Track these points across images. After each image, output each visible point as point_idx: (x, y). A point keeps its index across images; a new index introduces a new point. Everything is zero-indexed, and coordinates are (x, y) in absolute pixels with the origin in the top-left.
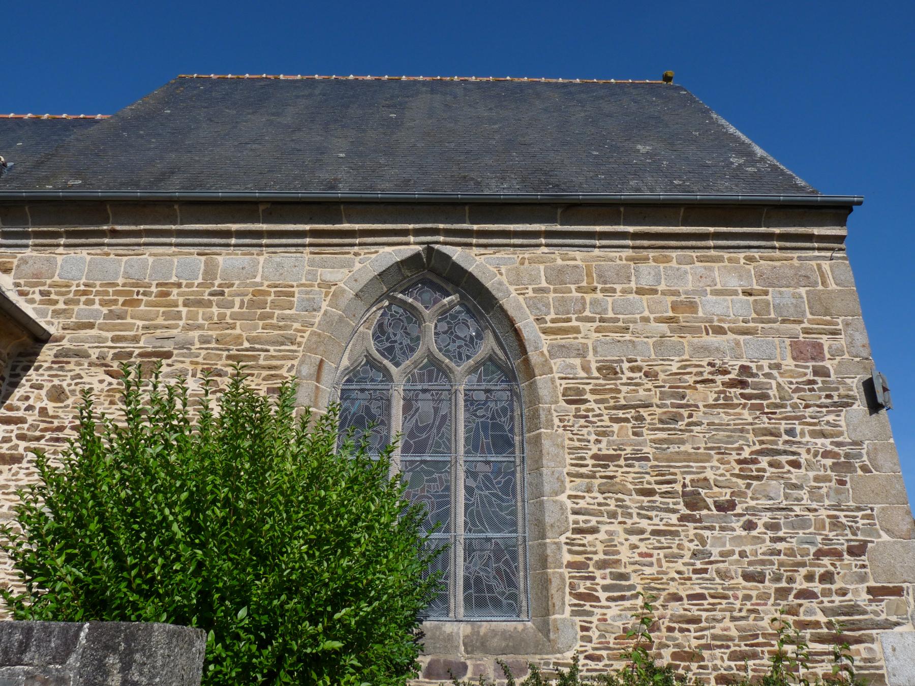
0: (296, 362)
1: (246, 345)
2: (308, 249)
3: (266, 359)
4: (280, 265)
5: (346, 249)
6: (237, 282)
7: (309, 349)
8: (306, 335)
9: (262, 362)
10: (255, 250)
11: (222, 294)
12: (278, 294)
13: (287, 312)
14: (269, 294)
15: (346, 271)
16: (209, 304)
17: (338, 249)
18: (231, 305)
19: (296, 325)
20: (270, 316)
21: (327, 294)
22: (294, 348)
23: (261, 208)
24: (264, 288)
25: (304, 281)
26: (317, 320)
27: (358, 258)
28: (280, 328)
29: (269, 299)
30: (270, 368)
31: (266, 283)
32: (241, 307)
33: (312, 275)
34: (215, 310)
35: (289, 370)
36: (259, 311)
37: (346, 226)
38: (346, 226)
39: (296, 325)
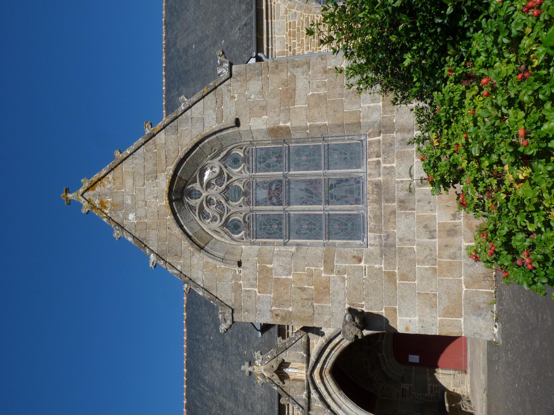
0: (315, 15)
2: (273, 20)
4: (279, 30)
5: (273, 7)
6: (286, 43)
7: (310, 12)
8: (305, 14)
10: (274, 39)
11: (290, 47)
12: (290, 27)
13: (297, 23)
14: (290, 31)
15: (281, 6)
16: (294, 51)
17: (273, 10)
18: (295, 43)
19: (302, 18)
20: (298, 29)
21: (290, 11)
22: (310, 17)
23: (258, 36)
24: (288, 33)
25: (285, 20)
26: (300, 12)
27: (276, 3)
28: (303, 24)
29: (292, 30)
31: (286, 33)
32: (295, 39)
34: (296, 48)
35: (318, 17)
36: (296, 32)
37: (264, 8)
38: (264, 8)
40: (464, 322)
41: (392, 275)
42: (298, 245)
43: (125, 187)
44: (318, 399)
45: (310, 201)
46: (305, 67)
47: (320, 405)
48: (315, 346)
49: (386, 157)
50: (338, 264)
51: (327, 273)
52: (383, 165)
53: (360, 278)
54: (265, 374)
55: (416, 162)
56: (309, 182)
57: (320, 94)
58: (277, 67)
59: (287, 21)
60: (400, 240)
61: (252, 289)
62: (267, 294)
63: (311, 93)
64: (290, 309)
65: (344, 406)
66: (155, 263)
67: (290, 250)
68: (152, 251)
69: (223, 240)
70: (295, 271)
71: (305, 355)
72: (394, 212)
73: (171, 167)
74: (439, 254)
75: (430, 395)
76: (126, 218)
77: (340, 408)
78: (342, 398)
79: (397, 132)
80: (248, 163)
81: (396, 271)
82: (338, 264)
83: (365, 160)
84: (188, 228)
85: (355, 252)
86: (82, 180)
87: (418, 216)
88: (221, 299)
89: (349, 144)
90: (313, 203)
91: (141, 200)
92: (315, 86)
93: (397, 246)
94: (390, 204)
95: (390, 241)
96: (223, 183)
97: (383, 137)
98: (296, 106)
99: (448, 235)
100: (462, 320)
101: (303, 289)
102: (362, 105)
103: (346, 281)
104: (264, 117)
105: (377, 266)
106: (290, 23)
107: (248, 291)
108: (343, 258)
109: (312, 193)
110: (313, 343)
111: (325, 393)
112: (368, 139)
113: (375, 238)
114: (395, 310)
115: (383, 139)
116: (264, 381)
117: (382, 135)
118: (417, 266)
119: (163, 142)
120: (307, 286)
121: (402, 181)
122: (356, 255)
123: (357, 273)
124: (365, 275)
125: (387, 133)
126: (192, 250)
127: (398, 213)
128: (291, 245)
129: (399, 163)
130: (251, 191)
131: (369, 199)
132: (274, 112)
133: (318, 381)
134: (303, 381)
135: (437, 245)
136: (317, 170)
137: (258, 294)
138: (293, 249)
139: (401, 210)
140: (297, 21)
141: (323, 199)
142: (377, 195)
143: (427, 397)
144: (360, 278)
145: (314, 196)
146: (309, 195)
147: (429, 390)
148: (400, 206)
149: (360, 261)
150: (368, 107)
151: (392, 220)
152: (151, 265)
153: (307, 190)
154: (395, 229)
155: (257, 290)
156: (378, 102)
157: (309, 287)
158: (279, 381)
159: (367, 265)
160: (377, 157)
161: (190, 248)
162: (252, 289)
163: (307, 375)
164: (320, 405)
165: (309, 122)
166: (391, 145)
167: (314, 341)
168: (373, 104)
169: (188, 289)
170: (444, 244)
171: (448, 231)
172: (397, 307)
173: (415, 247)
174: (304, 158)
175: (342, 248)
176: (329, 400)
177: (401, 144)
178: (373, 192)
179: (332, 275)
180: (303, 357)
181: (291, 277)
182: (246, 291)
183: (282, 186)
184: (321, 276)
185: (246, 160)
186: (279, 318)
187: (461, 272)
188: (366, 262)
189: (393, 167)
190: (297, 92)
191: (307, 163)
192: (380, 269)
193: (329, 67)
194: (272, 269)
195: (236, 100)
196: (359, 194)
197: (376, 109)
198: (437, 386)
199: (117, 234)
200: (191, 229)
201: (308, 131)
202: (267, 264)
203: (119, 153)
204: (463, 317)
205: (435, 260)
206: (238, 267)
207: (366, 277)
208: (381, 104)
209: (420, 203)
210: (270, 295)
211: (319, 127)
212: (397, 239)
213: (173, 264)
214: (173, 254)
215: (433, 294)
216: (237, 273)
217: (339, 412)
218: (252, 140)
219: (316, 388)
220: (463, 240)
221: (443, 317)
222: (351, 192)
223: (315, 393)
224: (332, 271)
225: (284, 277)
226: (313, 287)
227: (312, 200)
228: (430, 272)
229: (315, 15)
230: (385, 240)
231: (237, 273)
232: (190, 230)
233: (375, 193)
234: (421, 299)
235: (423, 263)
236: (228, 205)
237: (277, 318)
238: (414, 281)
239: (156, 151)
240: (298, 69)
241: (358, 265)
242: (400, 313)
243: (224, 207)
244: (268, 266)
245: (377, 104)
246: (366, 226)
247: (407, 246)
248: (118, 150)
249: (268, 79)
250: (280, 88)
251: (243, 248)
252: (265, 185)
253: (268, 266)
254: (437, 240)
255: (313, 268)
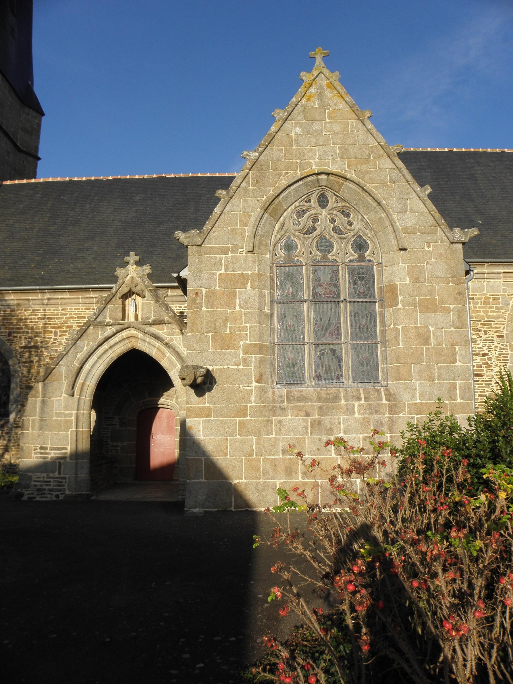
0: (505, 326)
1: (486, 319)
3: (495, 324)
6: (478, 294)
8: (507, 315)
9: (493, 326)
11: (473, 298)
12: (494, 298)
13: (498, 306)
18: (477, 303)
19: (503, 311)
22: (503, 320)
26: (510, 309)
28: (497, 312)
30: (496, 328)
31: (489, 294)
32: (481, 304)
33: (505, 290)
35: (503, 329)
36: (488, 305)
39: (503, 311)
40: (201, 482)
41: (244, 414)
42: (272, 315)
43: (330, 123)
44: (106, 335)
45: (318, 327)
46: (459, 324)
47: (100, 338)
48: (161, 332)
49: (365, 408)
50: (253, 359)
51: (243, 347)
52: (356, 404)
53: (240, 381)
54: (128, 278)
55: (359, 437)
56: (338, 327)
57: (431, 339)
58: (459, 294)
59: (501, 295)
60: (280, 422)
61: (223, 266)
62: (219, 283)
63: (431, 329)
64: (204, 308)
65: (100, 361)
66: (248, 157)
67: (266, 307)
68: (261, 154)
69: (275, 233)
70: (245, 314)
71: (150, 321)
72: (308, 415)
73: (354, 175)
74: (267, 459)
75: (109, 444)
76: (296, 125)
77: (99, 358)
78: (108, 359)
79: (389, 418)
80: (358, 261)
81: (248, 418)
82: (253, 359)
83: (362, 385)
84: (287, 194)
85: (266, 376)
86: (337, 73)
87: (305, 438)
88: (211, 232)
89: (378, 369)
90: (316, 332)
91: (317, 140)
92: (438, 334)
93: (273, 418)
94: (317, 411)
95: (279, 411)
96: (336, 232)
97: (385, 404)
98: (419, 314)
99: (286, 467)
100: (203, 480)
101: (225, 322)
102: (417, 382)
103: (236, 367)
104: (408, 279)
105: (253, 399)
106: (499, 298)
107: (221, 263)
108: (261, 362)
109: (326, 330)
110: (163, 330)
111: (112, 342)
112: (382, 389)
113: (281, 396)
114: (209, 416)
115: (383, 404)
116: (120, 277)
117: (387, 403)
118: (254, 438)
119: (382, 166)
120: (228, 326)
121: (340, 423)
122: (264, 377)
123: (245, 378)
124: (243, 387)
125: (389, 407)
126: (264, 199)
127: (308, 420)
128: (271, 308)
129: (358, 420)
130: (327, 264)
131: (321, 390)
132: (412, 290)
133: (124, 334)
134: (123, 318)
135: (276, 457)
136: (351, 336)
137: (218, 273)
138: (267, 310)
139: (311, 422)
140: (500, 306)
141: (320, 342)
142: (326, 399)
143: (107, 442)
144: (240, 381)
145: (323, 332)
146: (324, 327)
147: (115, 444)
148: (315, 421)
149: (257, 381)
150: (416, 389)
151: (300, 413)
152: (245, 153)
153: (329, 324)
154: (292, 416)
155: (222, 271)
156: (420, 399)
157: (228, 329)
158: (122, 294)
159: (253, 388)
160: (365, 398)
161: (265, 197)
162: (223, 266)
163: (130, 323)
164: (100, 337)
165: (402, 327)
166: (377, 412)
167: (165, 331)
168: (418, 394)
169: (221, 195)
170: (277, 463)
171: (290, 468)
172: (212, 418)
173: (274, 436)
174: (363, 322)
175: (269, 362)
176: (106, 346)
177: (377, 422)
178: (329, 394)
179: (241, 353)
180: (148, 318)
181: (238, 308)
182: (221, 260)
183: (333, 297)
184: (240, 341)
185: (361, 257)
186: (194, 296)
187: (249, 479)
188: (256, 387)
189: (354, 413)
190: (433, 315)
191: (358, 324)
192: (250, 402)
193: (457, 349)
194: (246, 288)
195: (426, 248)
196: (326, 379)
197: (414, 397)
198: (119, 451)
199: (279, 114)
200: (287, 197)
201: (392, 326)
202: (251, 283)
203: (369, 115)
204: (205, 481)
205: (261, 455)
206: (247, 250)
207: (241, 387)
208: (418, 401)
209: (318, 440)
210: (218, 286)
211: (397, 339)
212: (280, 418)
213: (247, 177)
214: (258, 178)
215: (227, 453)
216: (240, 250)
217: (94, 357)
218: (384, 264)
219: (118, 332)
220: (282, 481)
221: (205, 462)
222: (328, 371)
223: (112, 332)
224: (245, 352)
225: (238, 301)
226: (228, 332)
227: (319, 330)
228: (249, 451)
229: (505, 326)
230: (280, 406)
231: (240, 250)
232: (285, 196)
233: (328, 396)
234: (221, 441)
235: (258, 444)
236: (312, 238)
237: (193, 294)
238: (239, 435)
239: (372, 158)
240: (457, 315)
241: (253, 379)
242: (206, 420)
243: (310, 234)
244: (249, 284)
245: (418, 398)
246: (293, 387)
247: (274, 428)
248: (371, 114)
249: (447, 284)
250: (437, 297)
251: (267, 256)
252: (335, 279)
253: (249, 284)
254: (281, 457)
255: (248, 333)
